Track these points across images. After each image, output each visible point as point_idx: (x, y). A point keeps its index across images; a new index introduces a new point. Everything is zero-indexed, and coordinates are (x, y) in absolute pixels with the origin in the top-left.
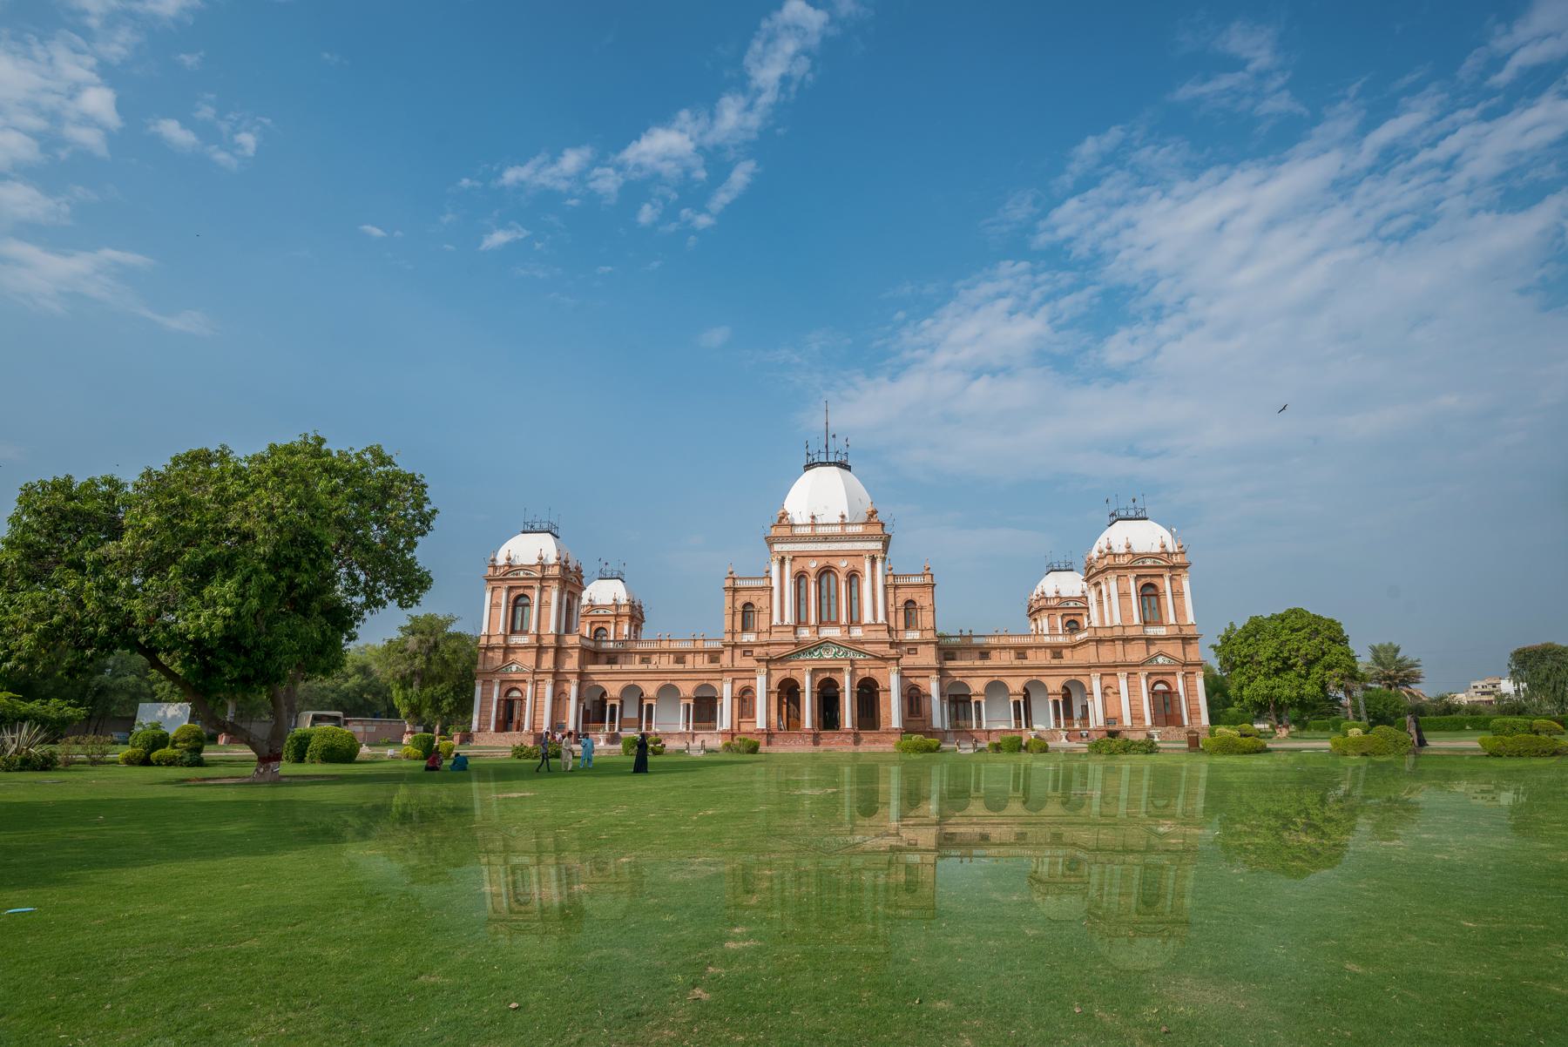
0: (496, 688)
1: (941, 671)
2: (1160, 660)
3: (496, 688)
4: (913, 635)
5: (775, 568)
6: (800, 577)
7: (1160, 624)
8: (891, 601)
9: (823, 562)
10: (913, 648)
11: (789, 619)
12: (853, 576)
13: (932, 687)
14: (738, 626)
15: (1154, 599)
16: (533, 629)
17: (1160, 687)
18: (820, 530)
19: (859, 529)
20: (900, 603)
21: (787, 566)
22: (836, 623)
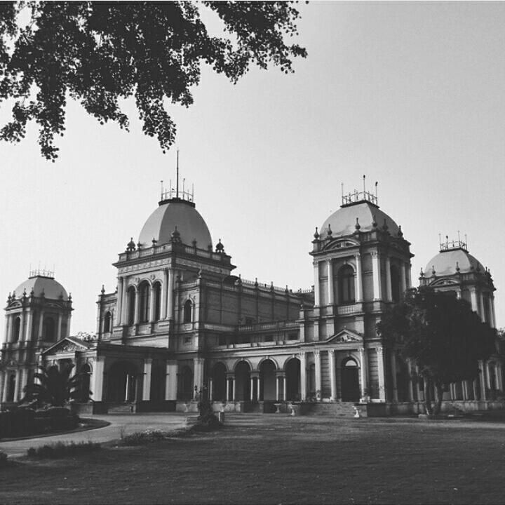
0: (6, 376)
1: (204, 352)
2: (345, 337)
3: (6, 376)
4: (189, 328)
5: (120, 285)
6: (131, 290)
7: (353, 302)
8: (177, 303)
9: (142, 277)
10: (188, 337)
11: (124, 321)
12: (157, 285)
13: (198, 368)
14: (103, 331)
15: (352, 278)
16: (20, 338)
17: (351, 363)
18: (145, 254)
19: (160, 250)
20: (183, 302)
21: (124, 284)
22: (147, 322)
